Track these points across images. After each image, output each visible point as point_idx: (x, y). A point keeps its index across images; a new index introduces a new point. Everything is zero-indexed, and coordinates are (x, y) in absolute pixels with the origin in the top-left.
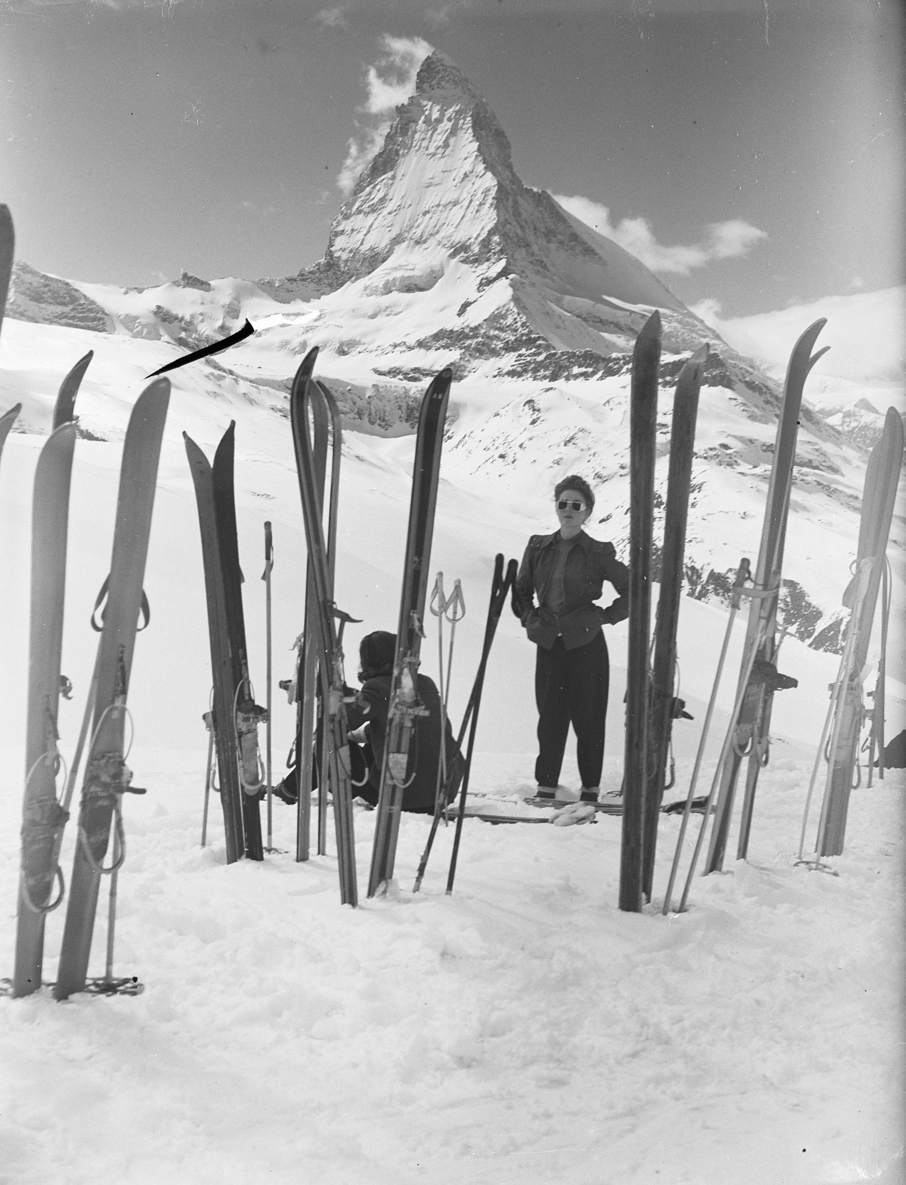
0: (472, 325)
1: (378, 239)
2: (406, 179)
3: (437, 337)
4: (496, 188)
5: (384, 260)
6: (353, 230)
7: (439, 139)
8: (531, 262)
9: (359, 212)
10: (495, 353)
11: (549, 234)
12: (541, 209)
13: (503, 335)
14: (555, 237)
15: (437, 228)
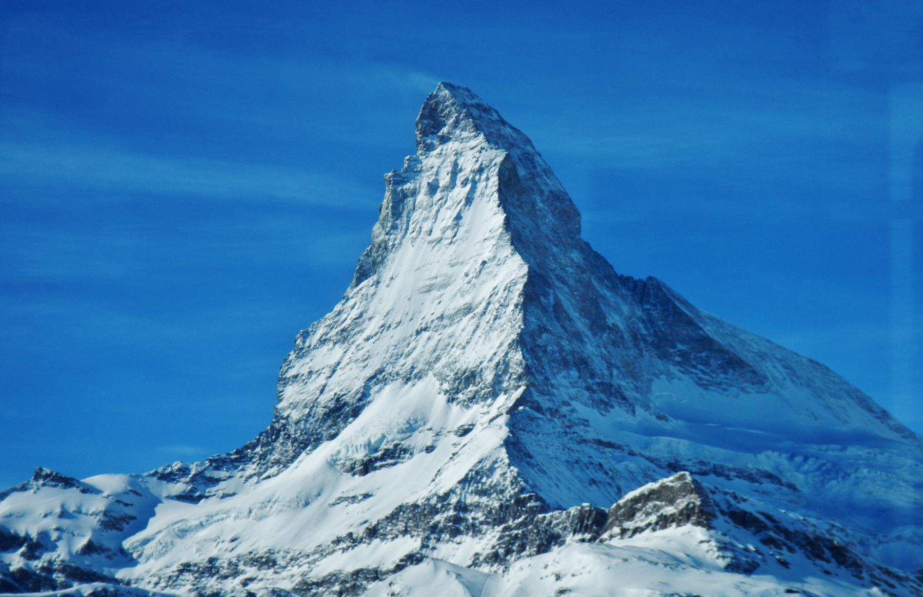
0: (441, 493)
1: (349, 381)
2: (397, 283)
3: (392, 518)
4: (525, 280)
5: (356, 412)
6: (310, 373)
7: (447, 216)
8: (588, 388)
9: (323, 342)
10: (475, 530)
11: (661, 346)
12: (647, 307)
13: (484, 500)
14: (674, 347)
15: (435, 354)
